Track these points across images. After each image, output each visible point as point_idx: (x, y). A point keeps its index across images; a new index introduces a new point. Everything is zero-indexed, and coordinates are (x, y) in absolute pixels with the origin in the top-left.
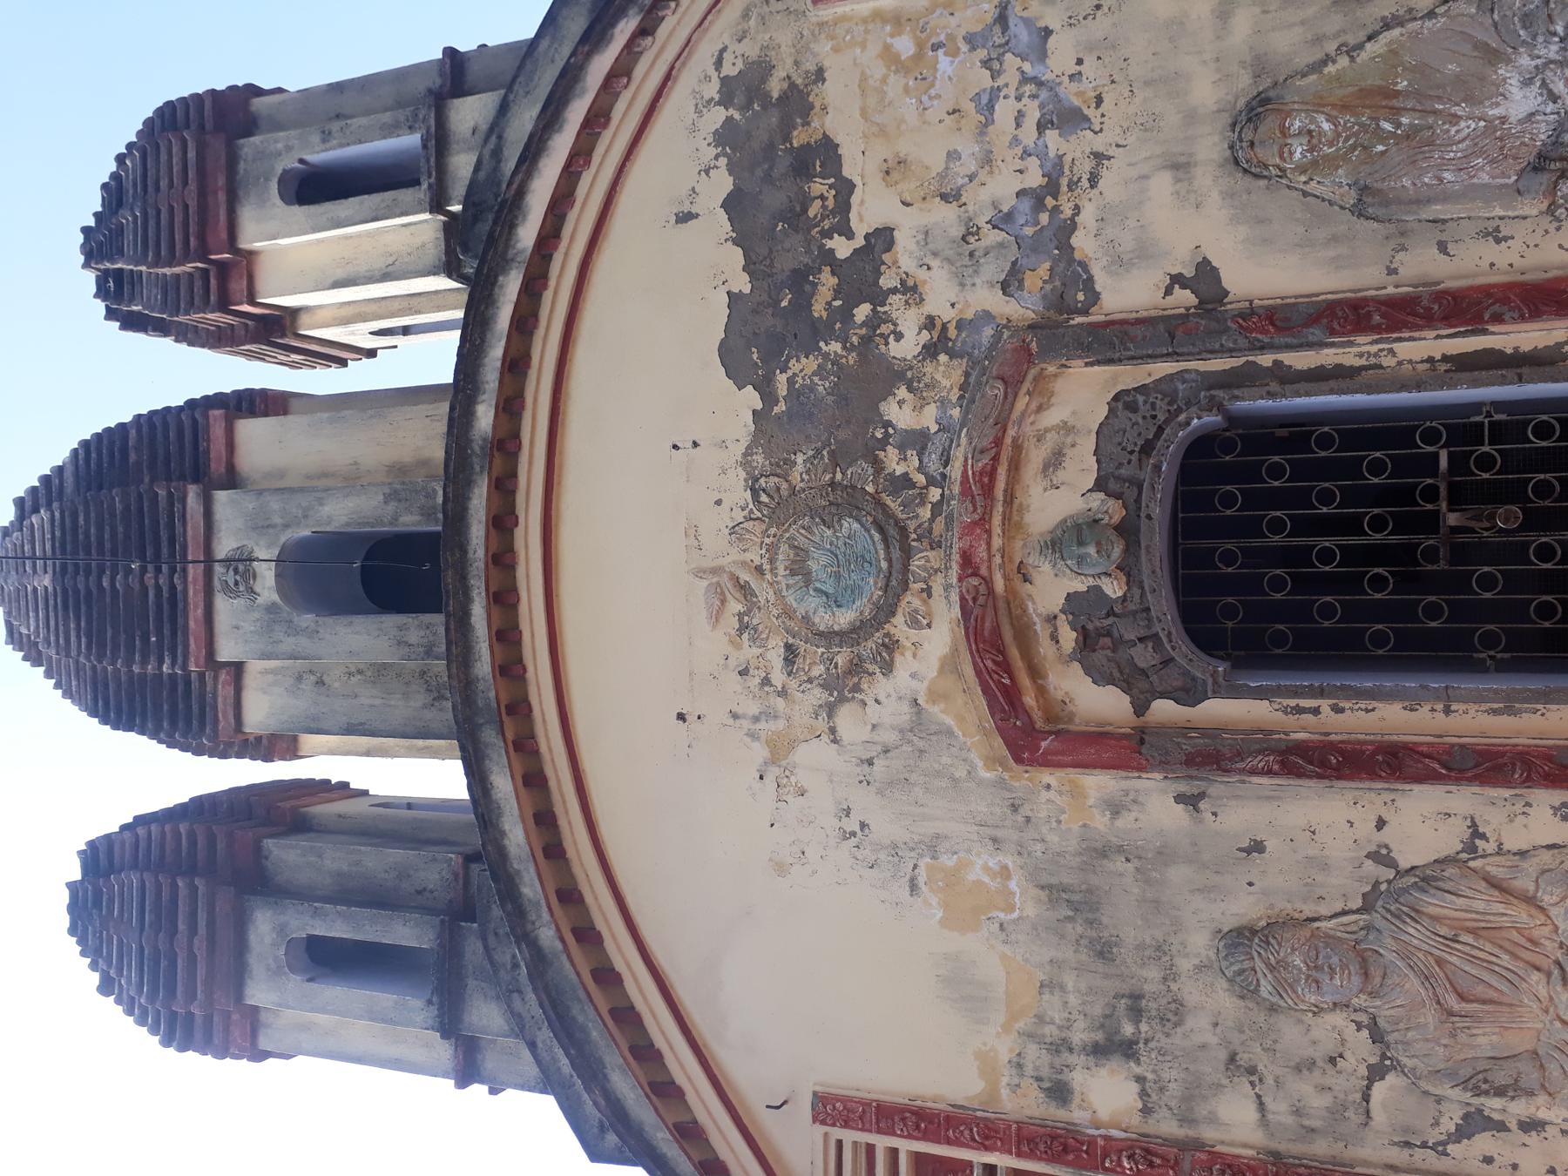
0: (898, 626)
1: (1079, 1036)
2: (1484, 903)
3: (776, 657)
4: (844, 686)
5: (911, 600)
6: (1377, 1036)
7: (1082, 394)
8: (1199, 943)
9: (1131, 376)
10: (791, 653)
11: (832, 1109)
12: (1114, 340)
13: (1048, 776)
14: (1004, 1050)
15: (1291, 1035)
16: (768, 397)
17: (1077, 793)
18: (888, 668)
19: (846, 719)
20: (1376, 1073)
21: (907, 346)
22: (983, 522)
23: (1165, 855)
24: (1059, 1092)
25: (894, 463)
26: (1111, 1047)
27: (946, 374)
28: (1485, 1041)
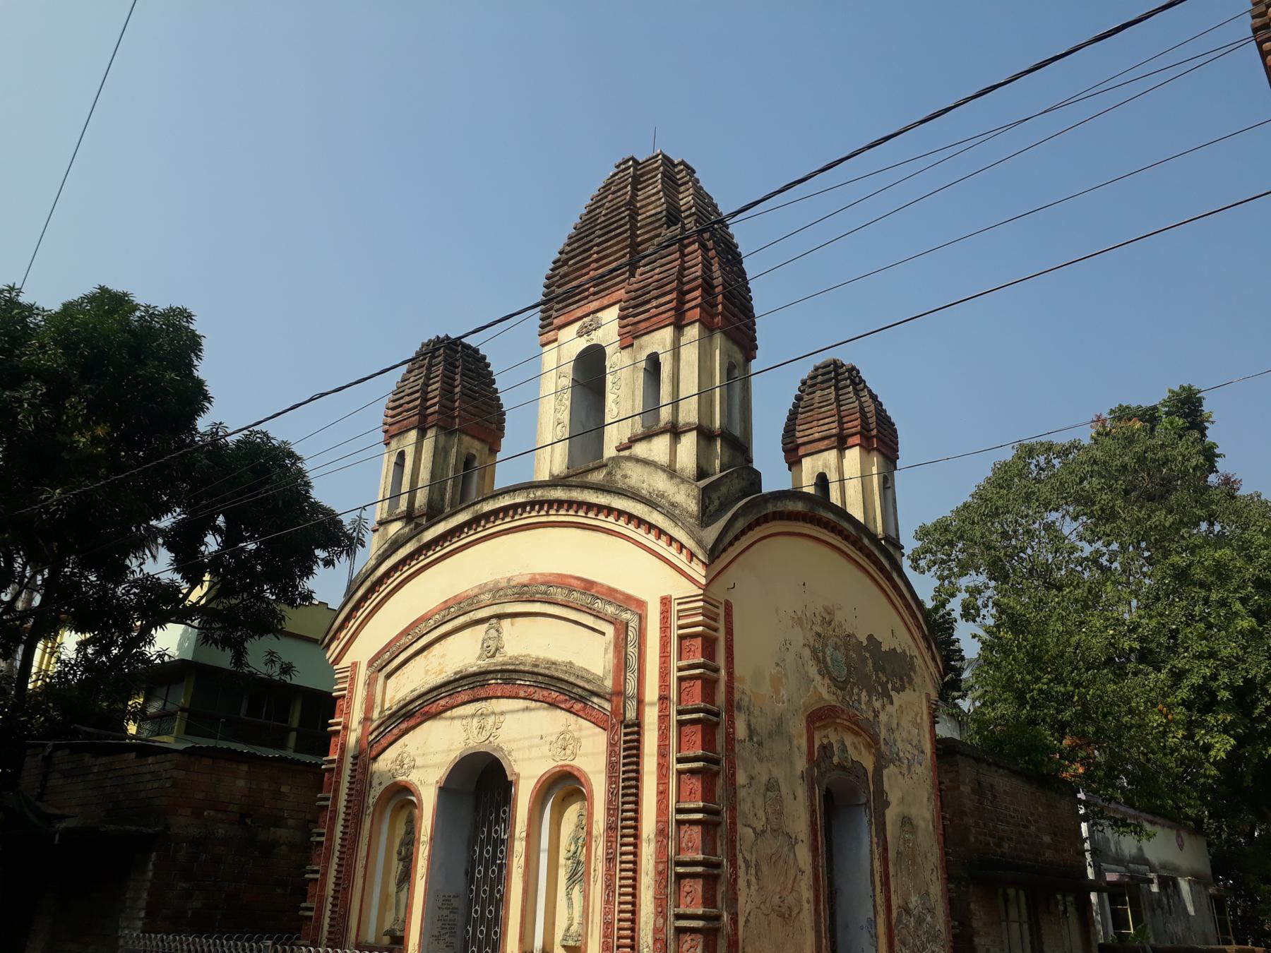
0: (827, 681)
1: (753, 721)
2: (792, 872)
3: (818, 629)
4: (814, 651)
5: (833, 689)
6: (763, 832)
7: (868, 762)
8: (775, 772)
9: (870, 775)
10: (818, 635)
11: (728, 607)
12: (878, 770)
13: (804, 724)
14: (747, 689)
15: (759, 802)
16: (866, 648)
17: (801, 736)
18: (819, 672)
19: (807, 653)
20: (754, 829)
21: (877, 705)
22: (849, 720)
23: (792, 764)
24: (739, 709)
25: (856, 690)
26: (751, 732)
27: (870, 715)
28: (765, 869)
